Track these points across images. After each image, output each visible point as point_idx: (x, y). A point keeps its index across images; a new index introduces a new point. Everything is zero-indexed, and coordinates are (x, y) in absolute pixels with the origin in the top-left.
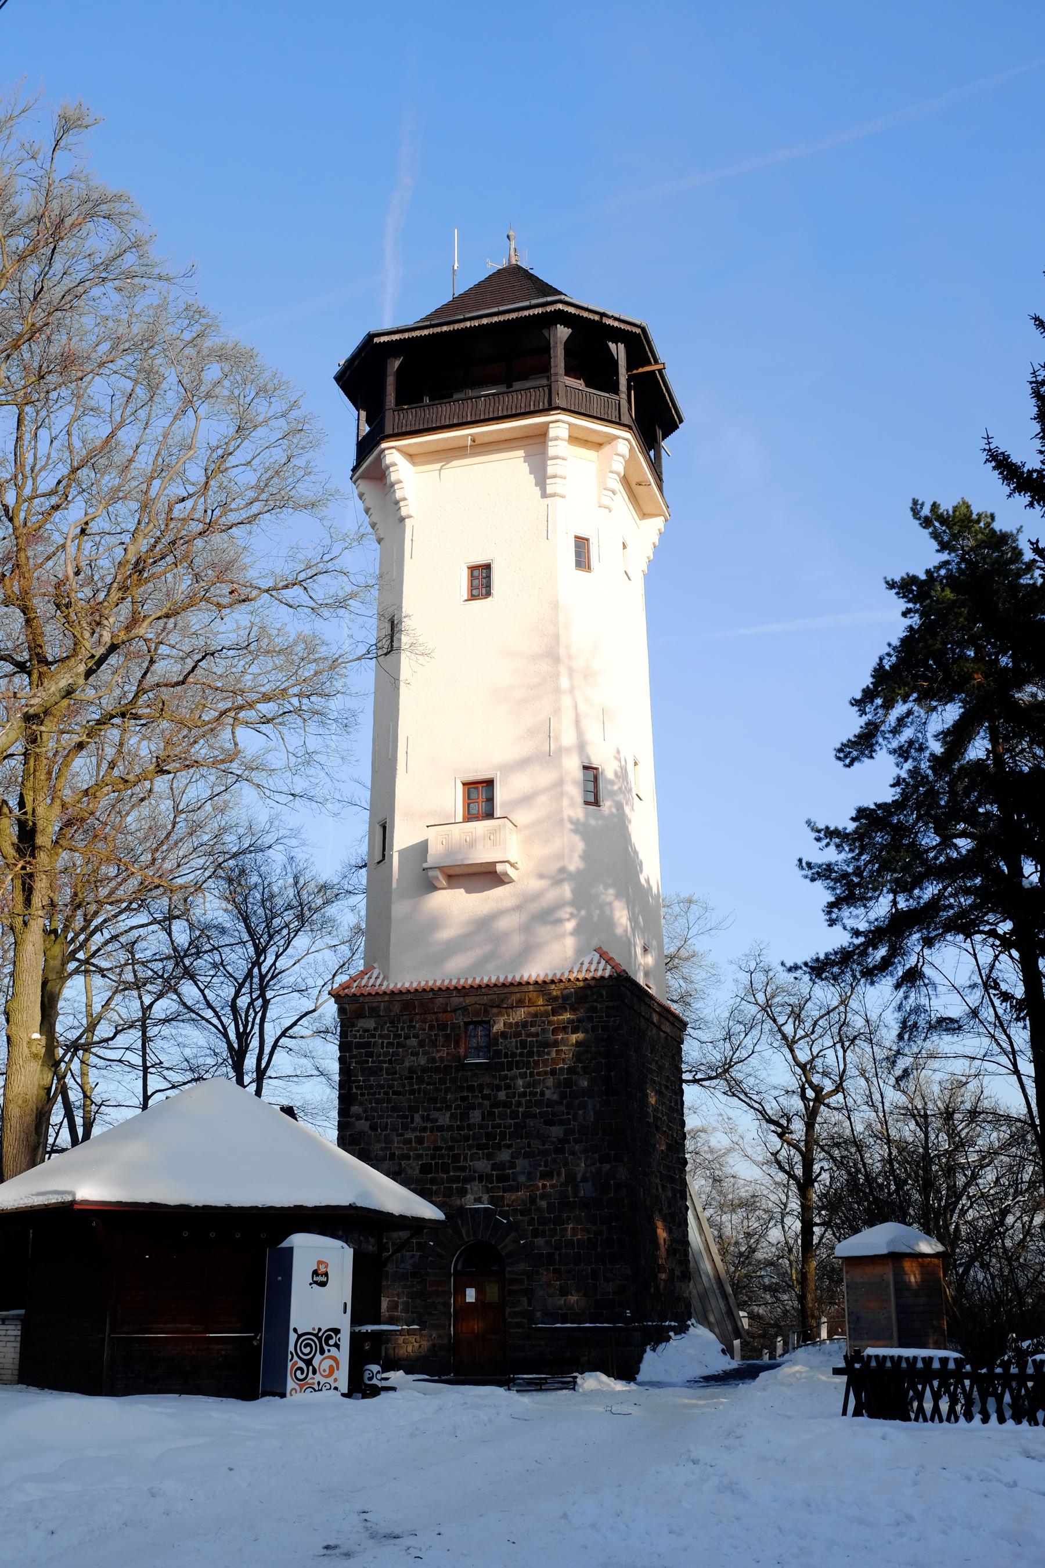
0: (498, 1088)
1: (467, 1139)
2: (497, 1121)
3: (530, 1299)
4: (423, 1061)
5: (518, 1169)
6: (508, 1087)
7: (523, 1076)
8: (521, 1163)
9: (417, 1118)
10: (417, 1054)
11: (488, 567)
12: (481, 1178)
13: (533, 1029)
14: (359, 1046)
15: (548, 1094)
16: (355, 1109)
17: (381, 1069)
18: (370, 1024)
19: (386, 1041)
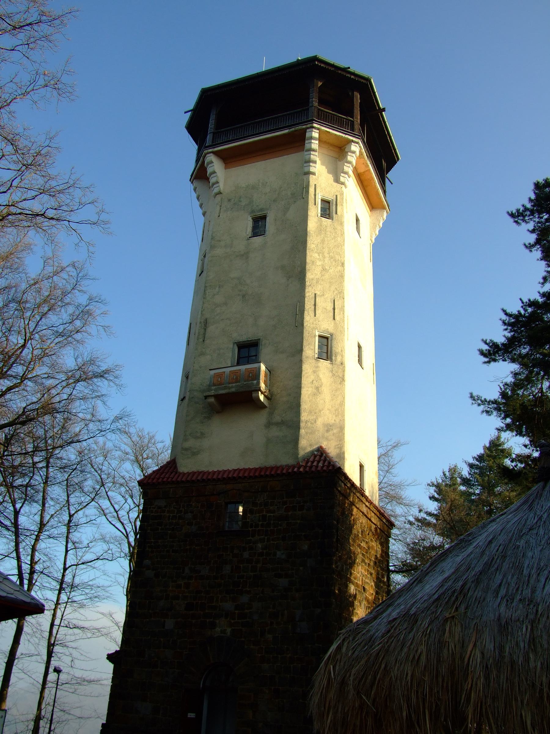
13: (271, 508)
15: (278, 553)
16: (147, 562)
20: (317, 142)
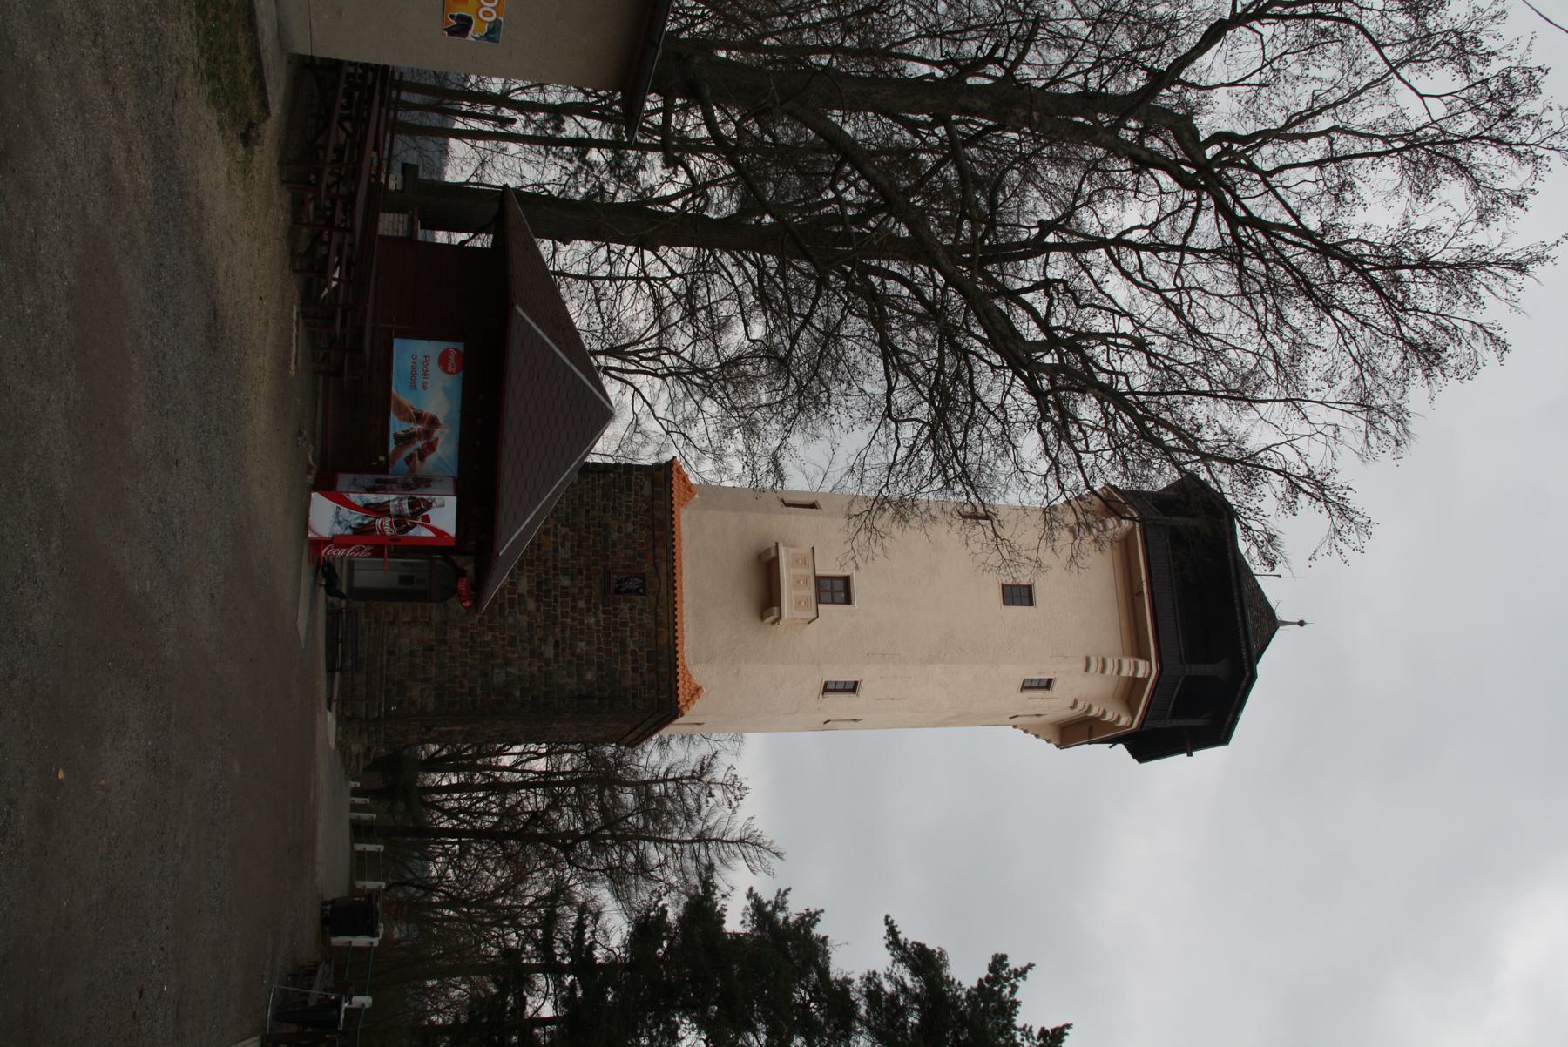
0: (588, 602)
1: (546, 572)
2: (560, 600)
3: (409, 623)
4: (615, 536)
5: (519, 616)
6: (589, 610)
7: (597, 622)
8: (524, 620)
9: (565, 530)
10: (620, 531)
11: (1030, 602)
12: (511, 584)
14: (629, 481)
15: (583, 644)
17: (608, 500)
18: (647, 491)
19: (632, 504)
20: (1131, 675)
